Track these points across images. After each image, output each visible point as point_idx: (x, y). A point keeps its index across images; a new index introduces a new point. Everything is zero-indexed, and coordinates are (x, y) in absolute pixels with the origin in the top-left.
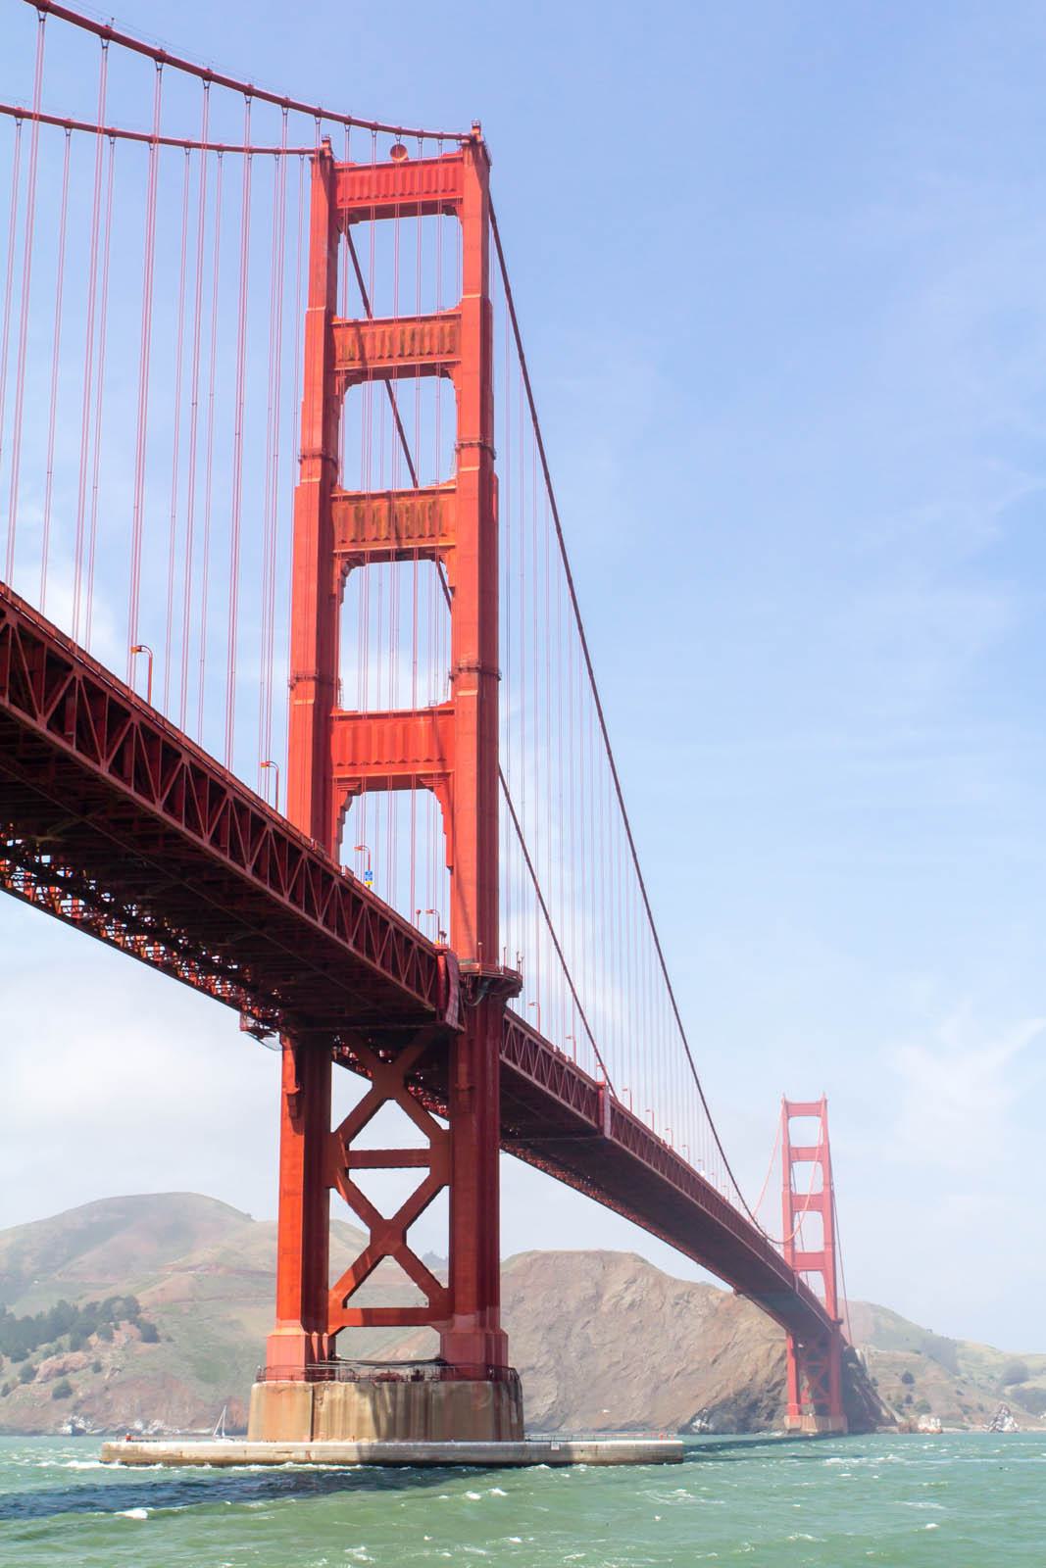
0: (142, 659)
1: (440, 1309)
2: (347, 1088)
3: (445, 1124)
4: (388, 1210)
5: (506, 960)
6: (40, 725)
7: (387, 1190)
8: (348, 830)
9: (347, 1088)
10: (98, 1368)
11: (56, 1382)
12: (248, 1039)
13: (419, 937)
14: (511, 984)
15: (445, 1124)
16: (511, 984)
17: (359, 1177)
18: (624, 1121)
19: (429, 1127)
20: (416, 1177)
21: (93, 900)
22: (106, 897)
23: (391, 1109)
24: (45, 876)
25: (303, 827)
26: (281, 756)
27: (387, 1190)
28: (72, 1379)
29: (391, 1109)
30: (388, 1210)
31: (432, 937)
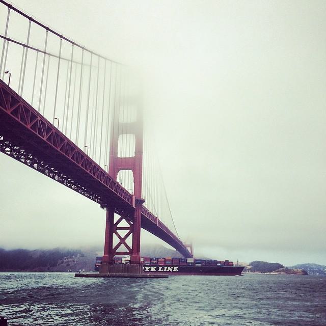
0: (87, 148)
1: (131, 252)
2: (117, 217)
3: (132, 223)
4: (123, 237)
5: (143, 197)
6: (70, 158)
7: (123, 233)
8: (118, 176)
9: (117, 217)
10: (74, 261)
11: (67, 263)
12: (101, 209)
13: (129, 193)
14: (143, 201)
15: (132, 223)
16: (143, 201)
17: (118, 231)
18: (160, 223)
19: (129, 223)
20: (127, 231)
21: (77, 186)
22: (79, 186)
23: (124, 220)
24: (70, 182)
25: (111, 175)
26: (108, 164)
27: (123, 233)
28: (70, 263)
29: (124, 220)
30: (123, 237)
31: (131, 193)
